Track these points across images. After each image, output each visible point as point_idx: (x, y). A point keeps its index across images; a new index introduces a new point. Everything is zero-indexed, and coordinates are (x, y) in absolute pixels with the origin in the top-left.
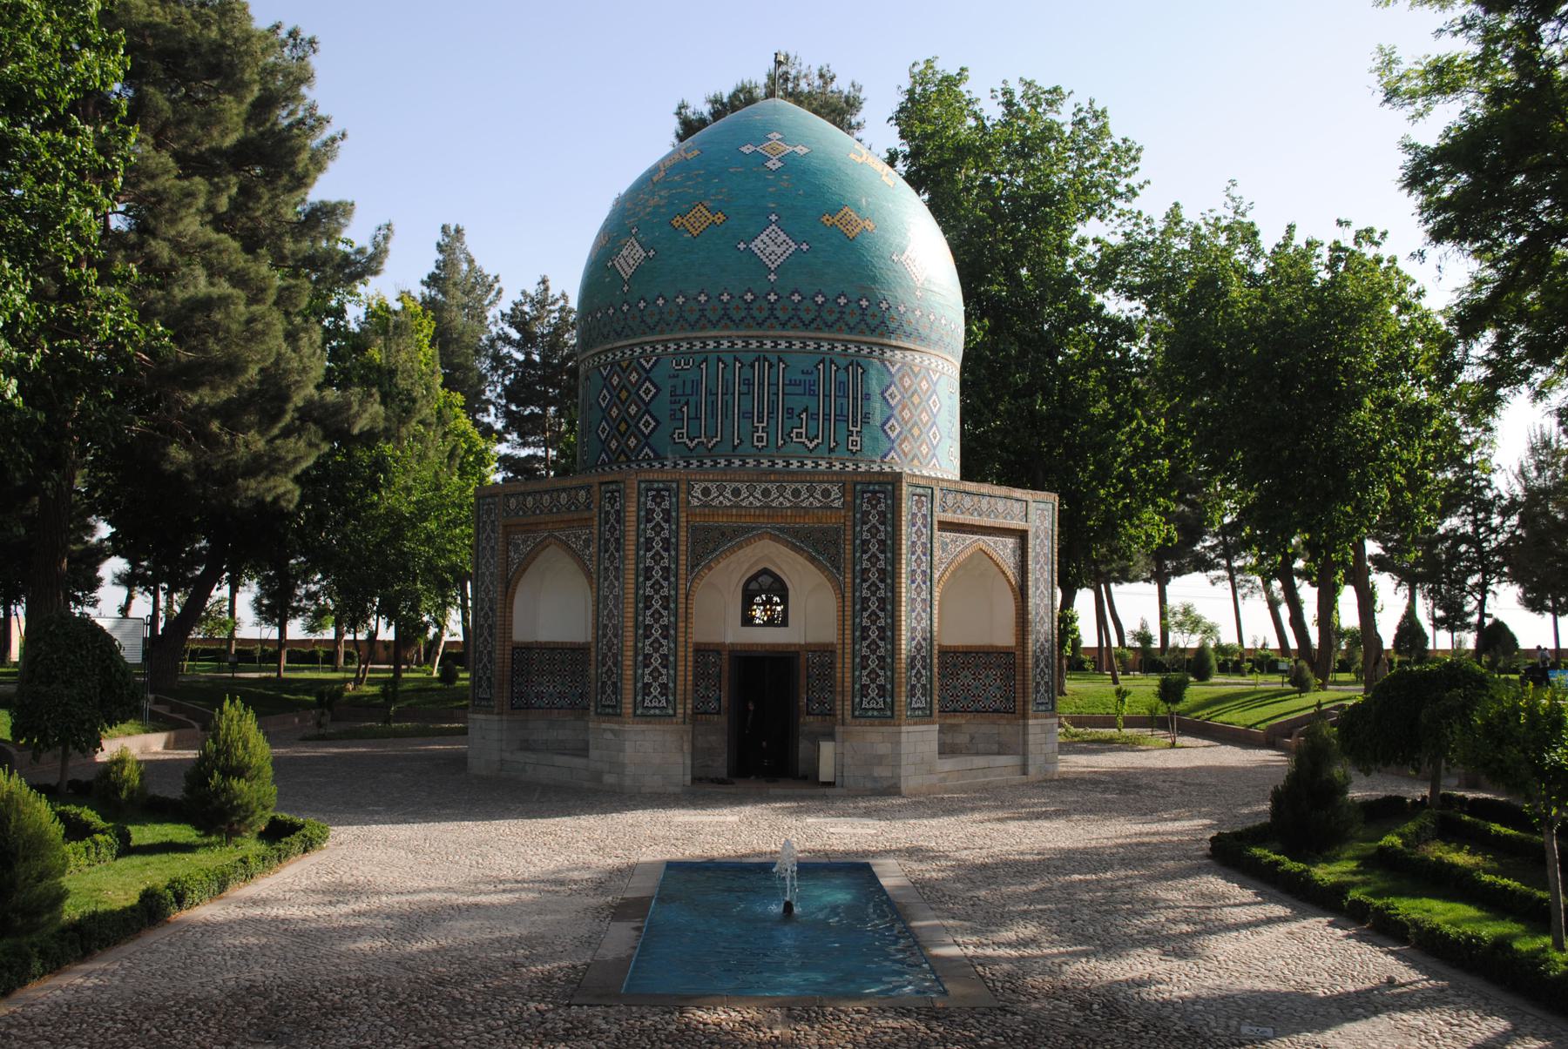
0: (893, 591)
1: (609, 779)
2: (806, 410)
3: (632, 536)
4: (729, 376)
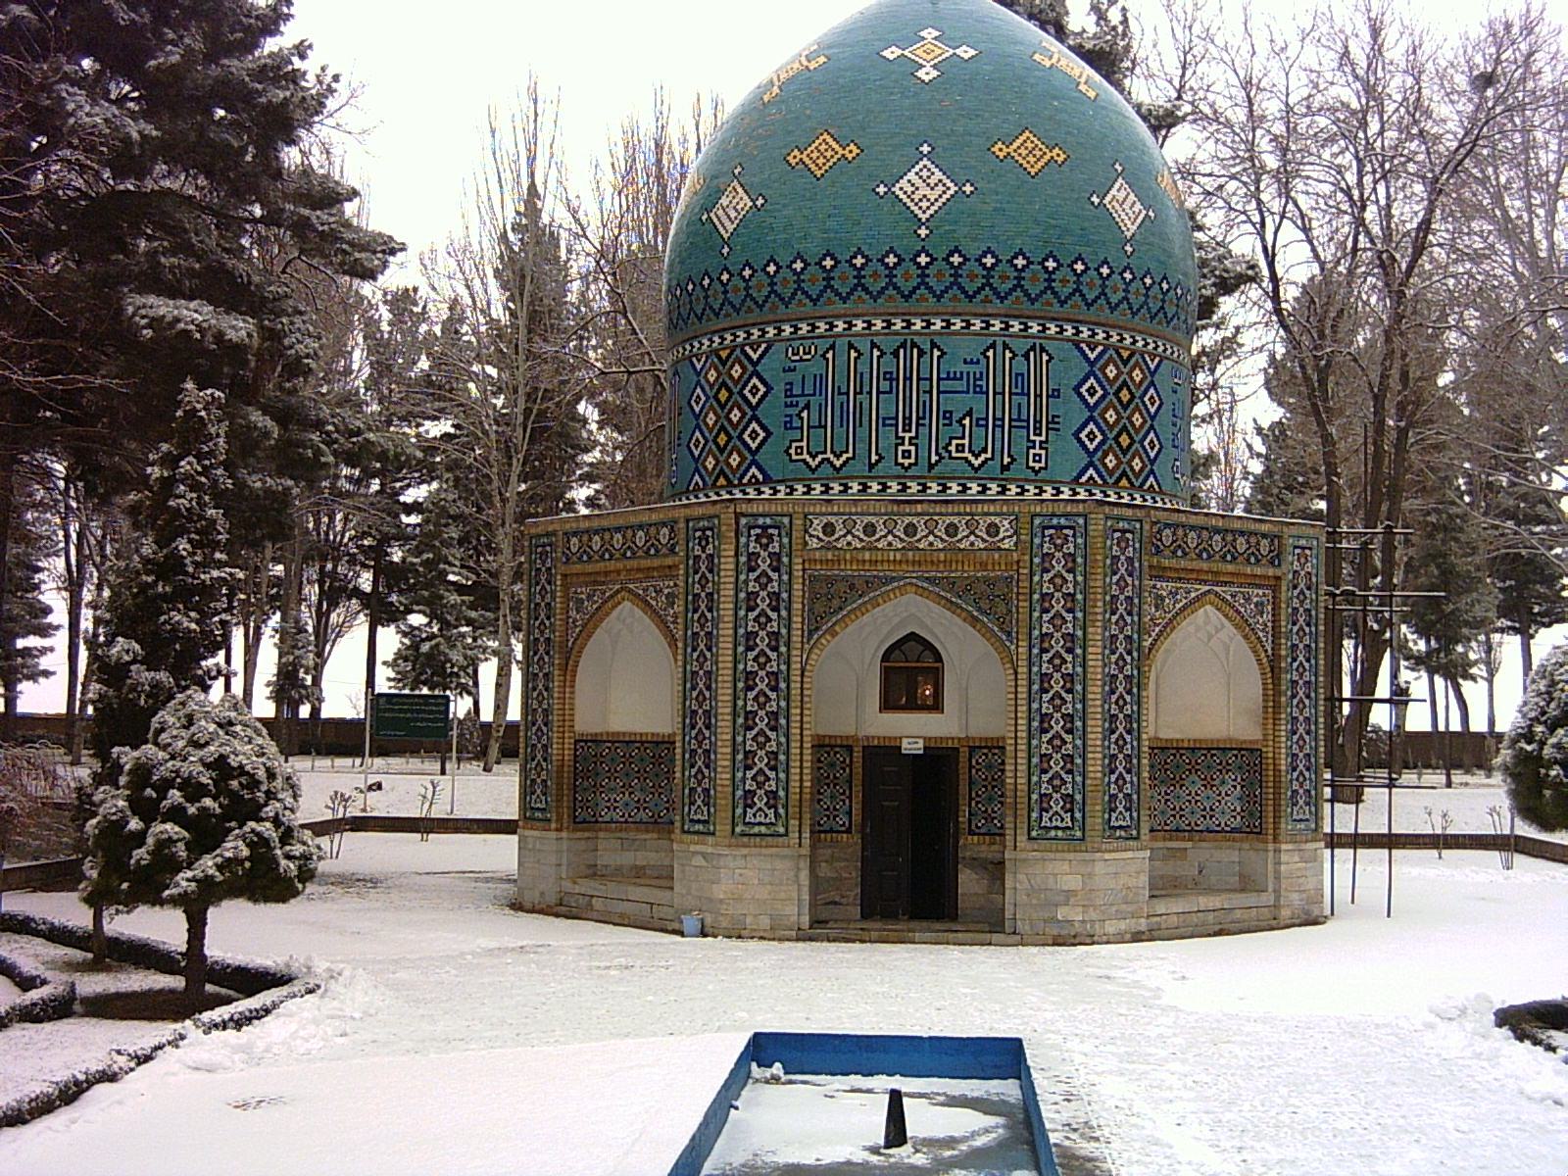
0: (1084, 666)
2: (970, 413)
3: (728, 591)
4: (863, 368)
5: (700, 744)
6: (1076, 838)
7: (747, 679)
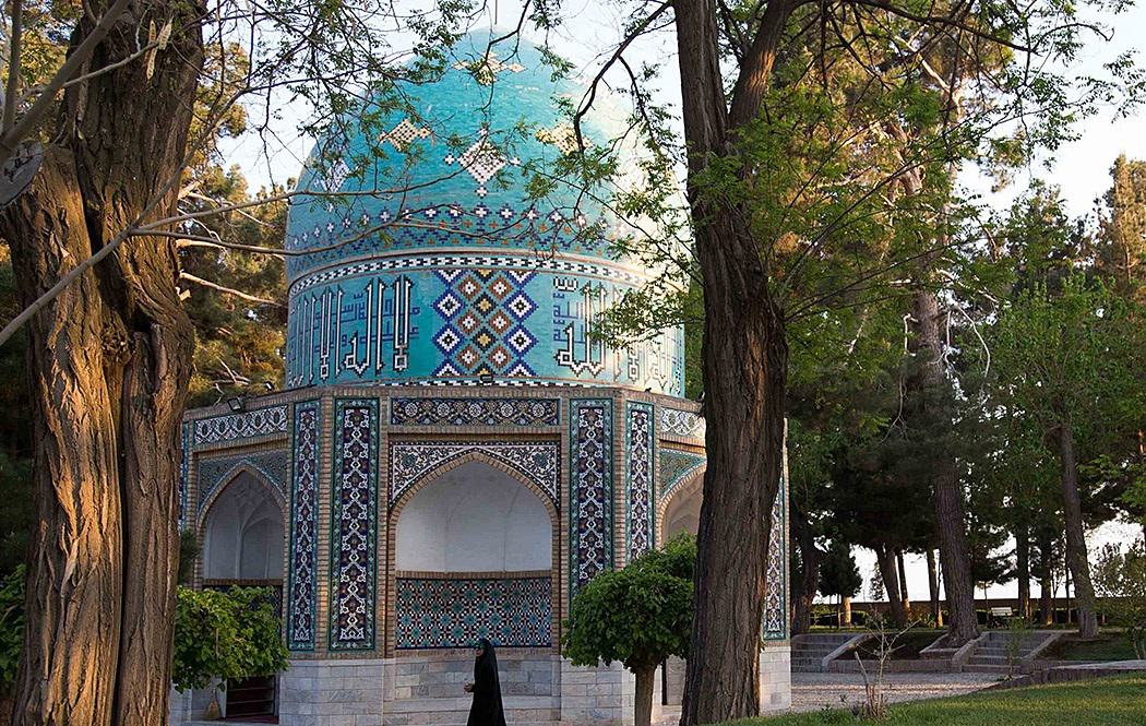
5: (303, 579)
7: (342, 526)
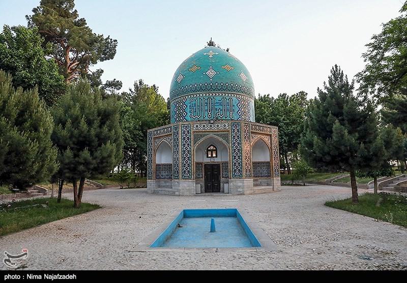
1: (177, 193)
6: (240, 176)
